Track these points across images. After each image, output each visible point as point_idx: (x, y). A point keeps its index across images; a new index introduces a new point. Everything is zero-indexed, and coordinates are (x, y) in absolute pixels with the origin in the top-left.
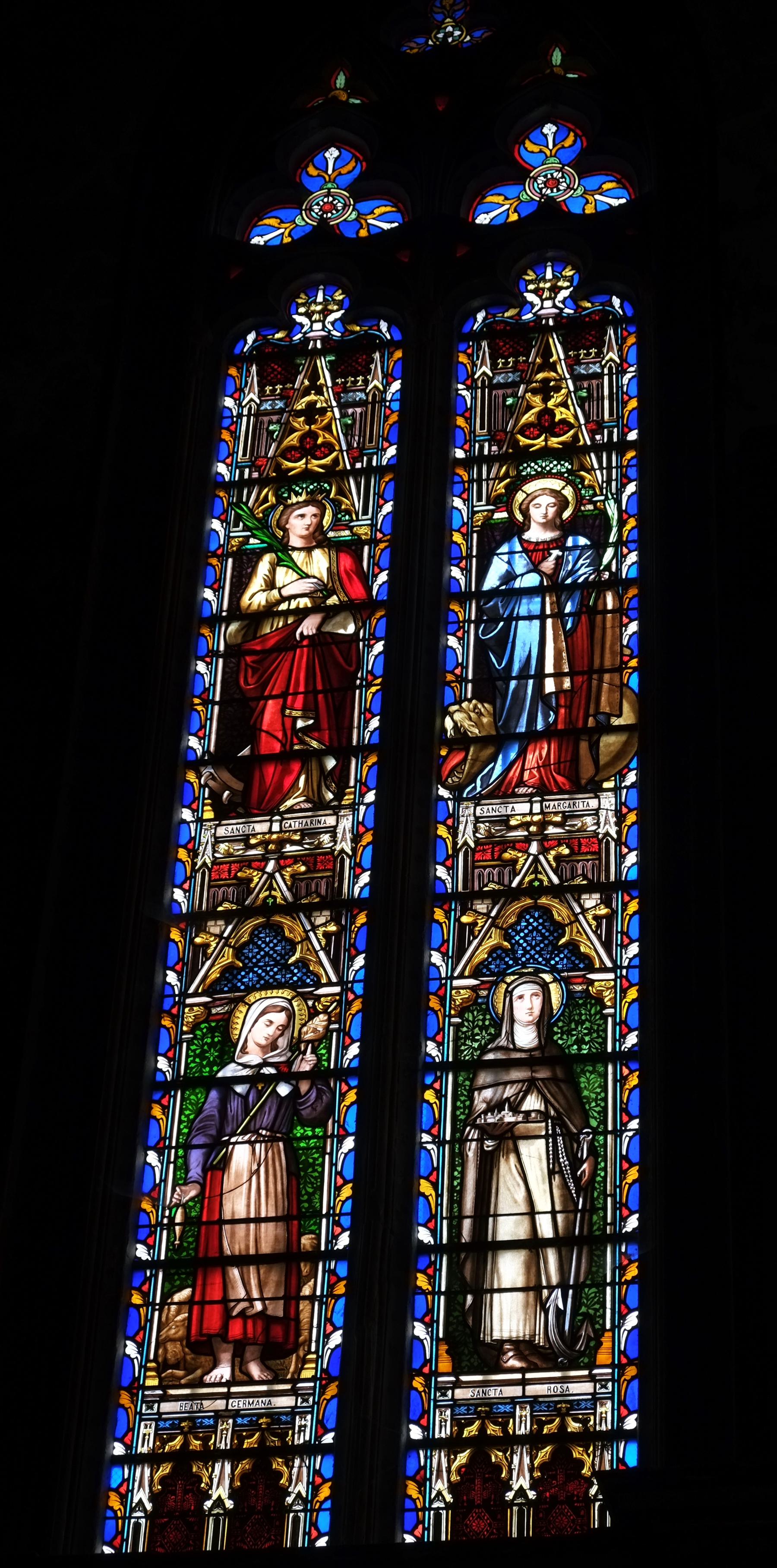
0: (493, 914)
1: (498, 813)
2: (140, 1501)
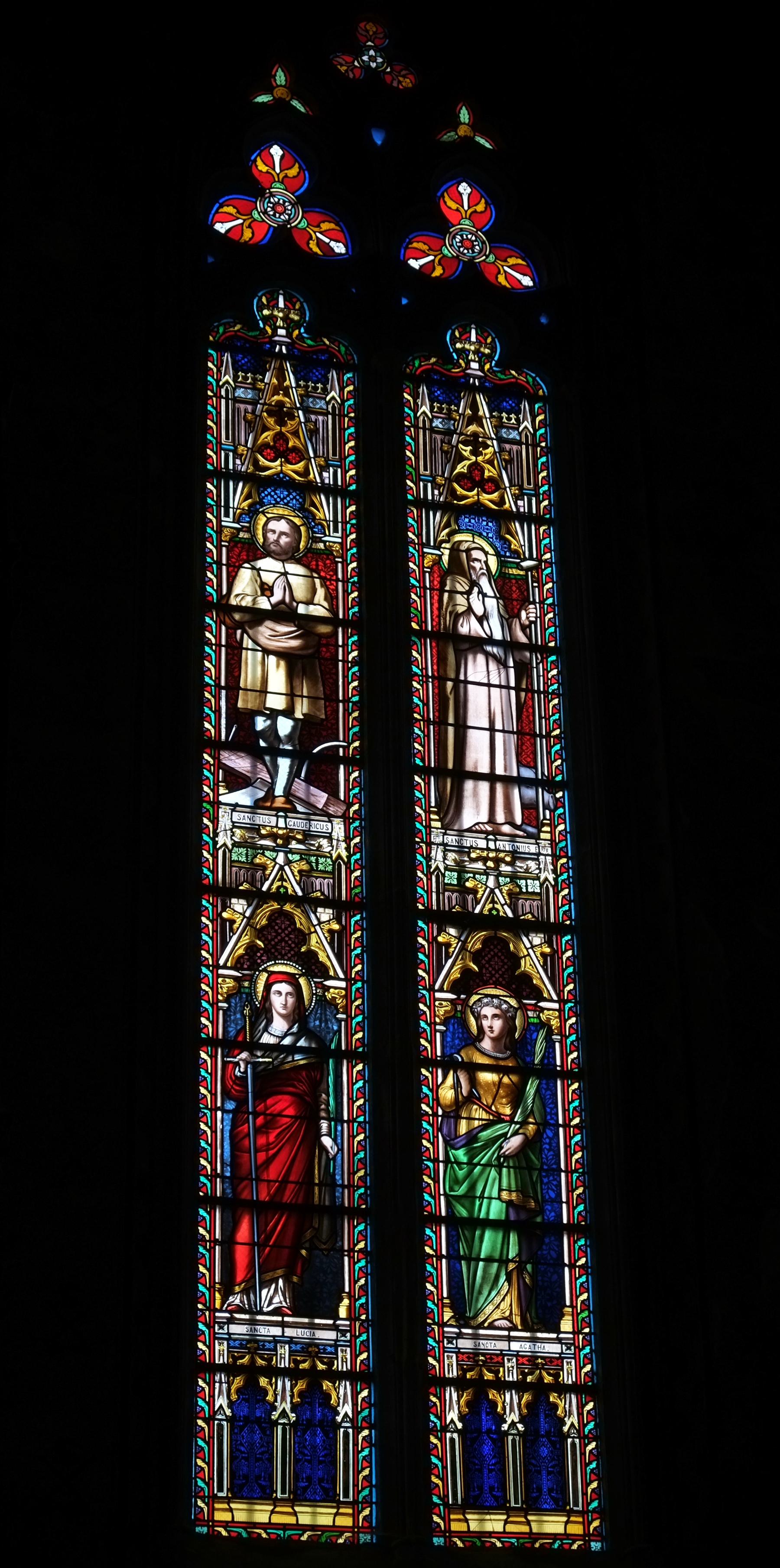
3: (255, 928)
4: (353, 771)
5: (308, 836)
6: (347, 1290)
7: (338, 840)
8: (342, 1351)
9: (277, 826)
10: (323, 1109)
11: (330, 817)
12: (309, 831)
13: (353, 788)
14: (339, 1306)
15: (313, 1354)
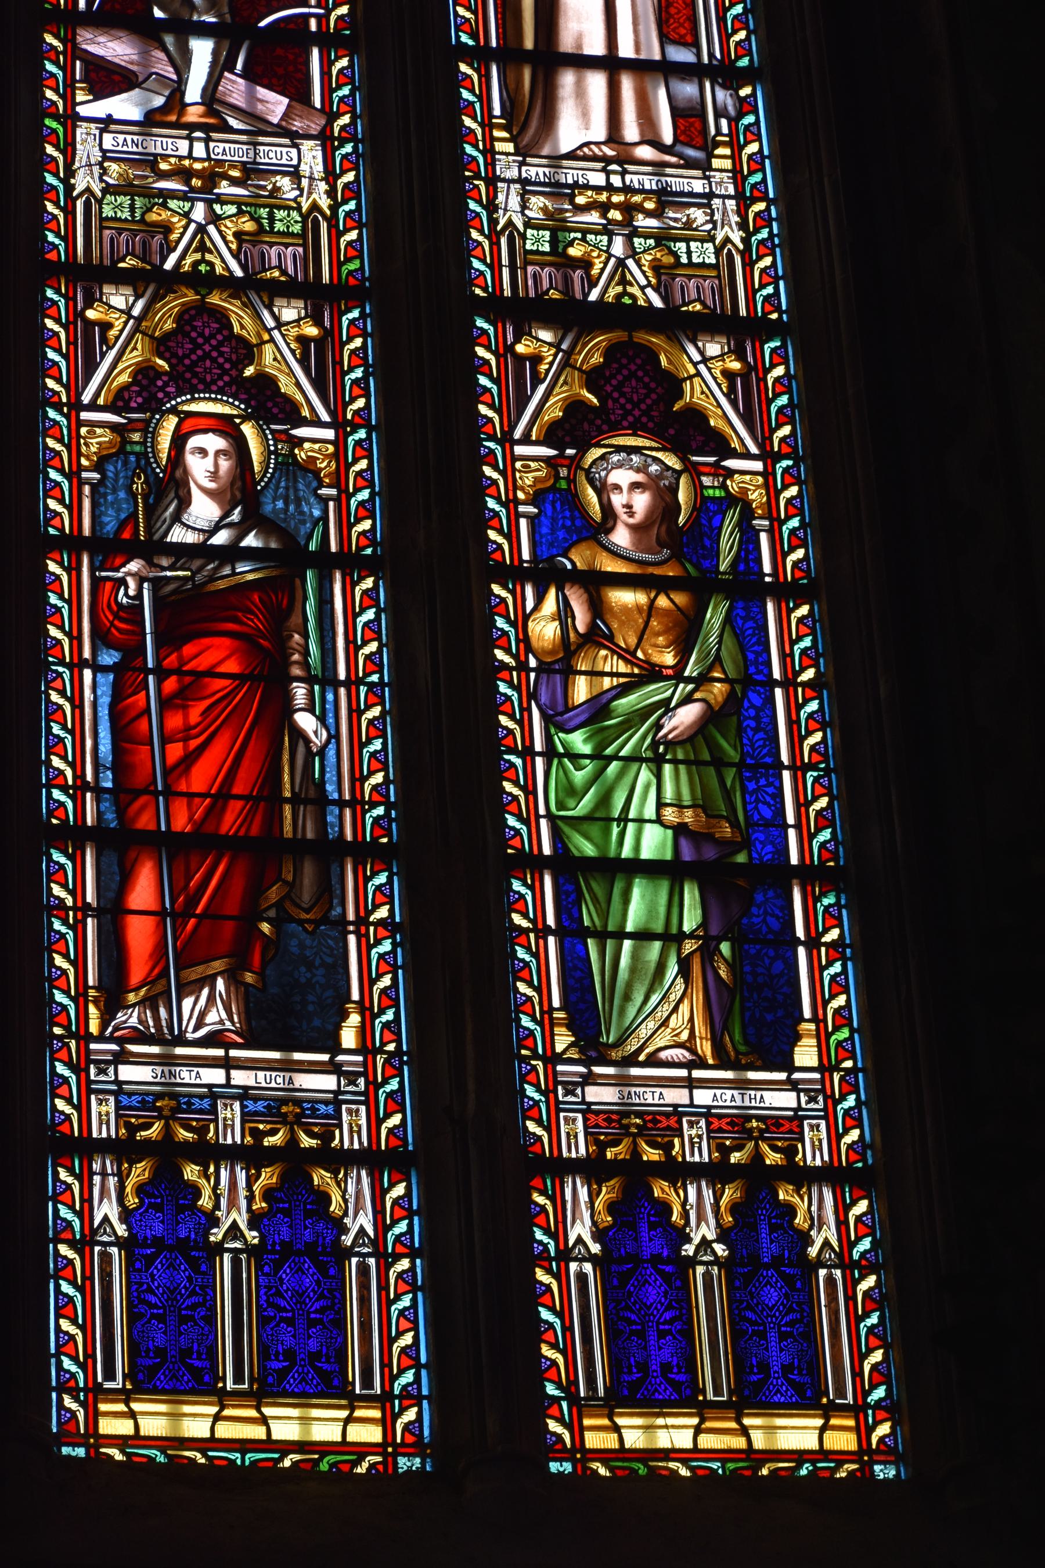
0: (136, 312)
1: (140, 150)
2: (106, 1219)
3: (152, 337)
4: (338, 58)
5: (251, 171)
6: (355, 995)
7: (311, 178)
8: (350, 1112)
9: (190, 156)
10: (296, 662)
11: (294, 138)
12: (255, 163)
13: (339, 87)
14: (340, 1028)
15: (290, 1118)
